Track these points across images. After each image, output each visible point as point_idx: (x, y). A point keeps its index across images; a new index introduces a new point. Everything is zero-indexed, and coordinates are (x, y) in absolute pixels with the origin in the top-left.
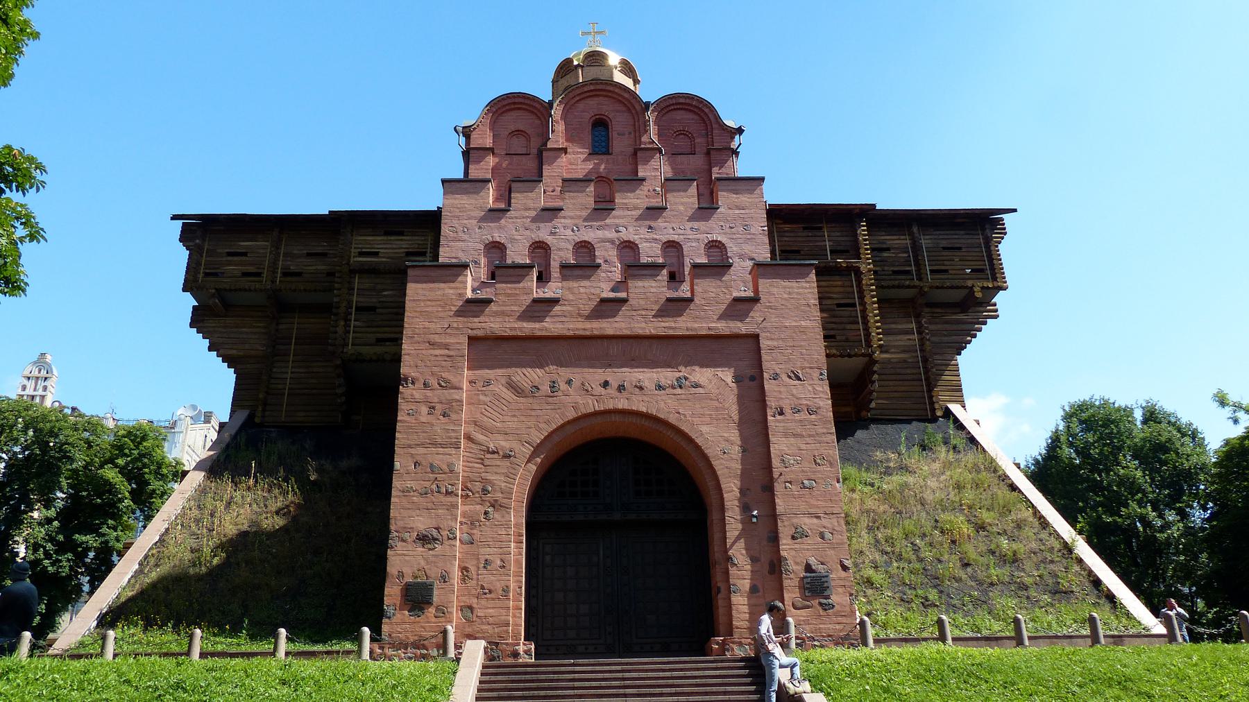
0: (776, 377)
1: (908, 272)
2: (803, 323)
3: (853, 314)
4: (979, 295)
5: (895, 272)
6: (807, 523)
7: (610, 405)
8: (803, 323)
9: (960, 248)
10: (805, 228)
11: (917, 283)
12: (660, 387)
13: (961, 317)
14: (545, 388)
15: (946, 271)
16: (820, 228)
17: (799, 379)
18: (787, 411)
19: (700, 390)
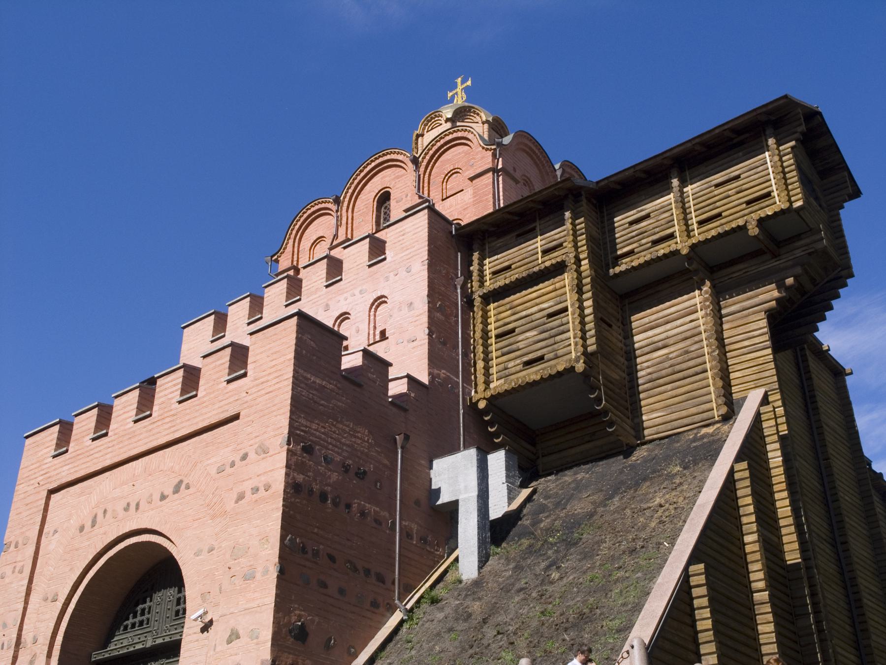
0: (244, 457)
1: (671, 236)
2: (277, 386)
3: (564, 320)
4: (753, 231)
5: (655, 243)
6: (243, 625)
7: (127, 529)
8: (277, 386)
9: (737, 177)
10: (518, 236)
11: (673, 247)
12: (163, 497)
13: (774, 263)
14: (88, 524)
15: (719, 215)
16: (534, 229)
17: (265, 452)
18: (248, 494)
19: (191, 490)
